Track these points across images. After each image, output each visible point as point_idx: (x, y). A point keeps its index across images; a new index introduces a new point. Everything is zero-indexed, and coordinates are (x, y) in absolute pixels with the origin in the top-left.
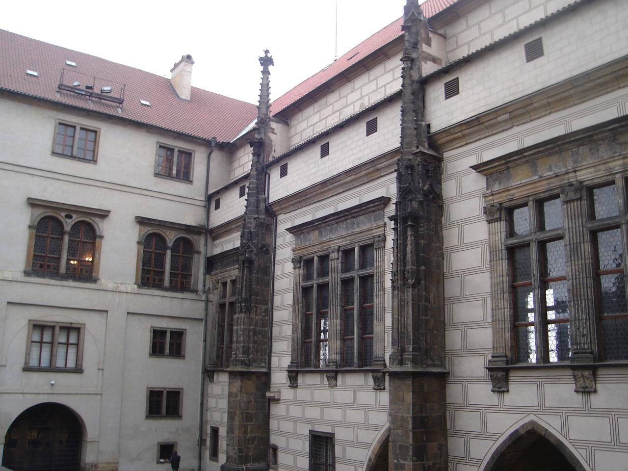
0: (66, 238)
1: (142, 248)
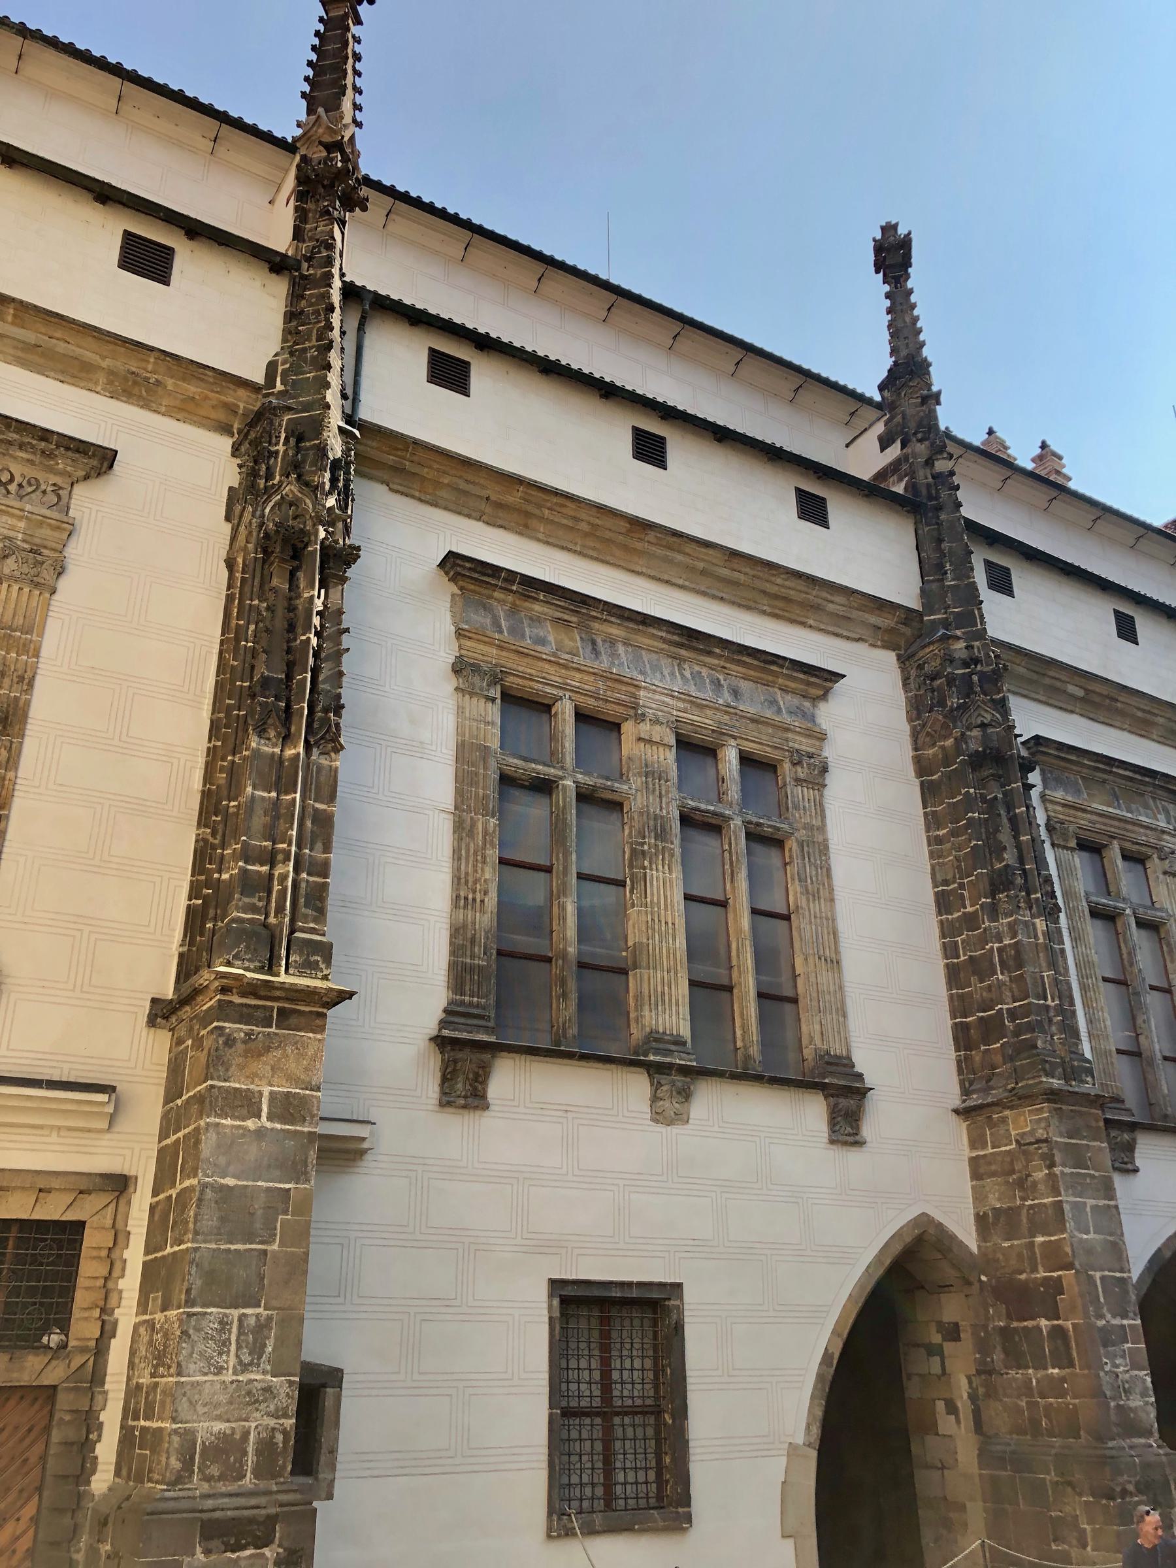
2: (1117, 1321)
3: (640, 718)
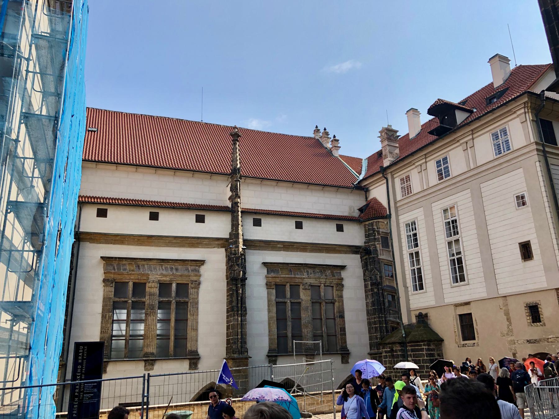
3: (149, 282)
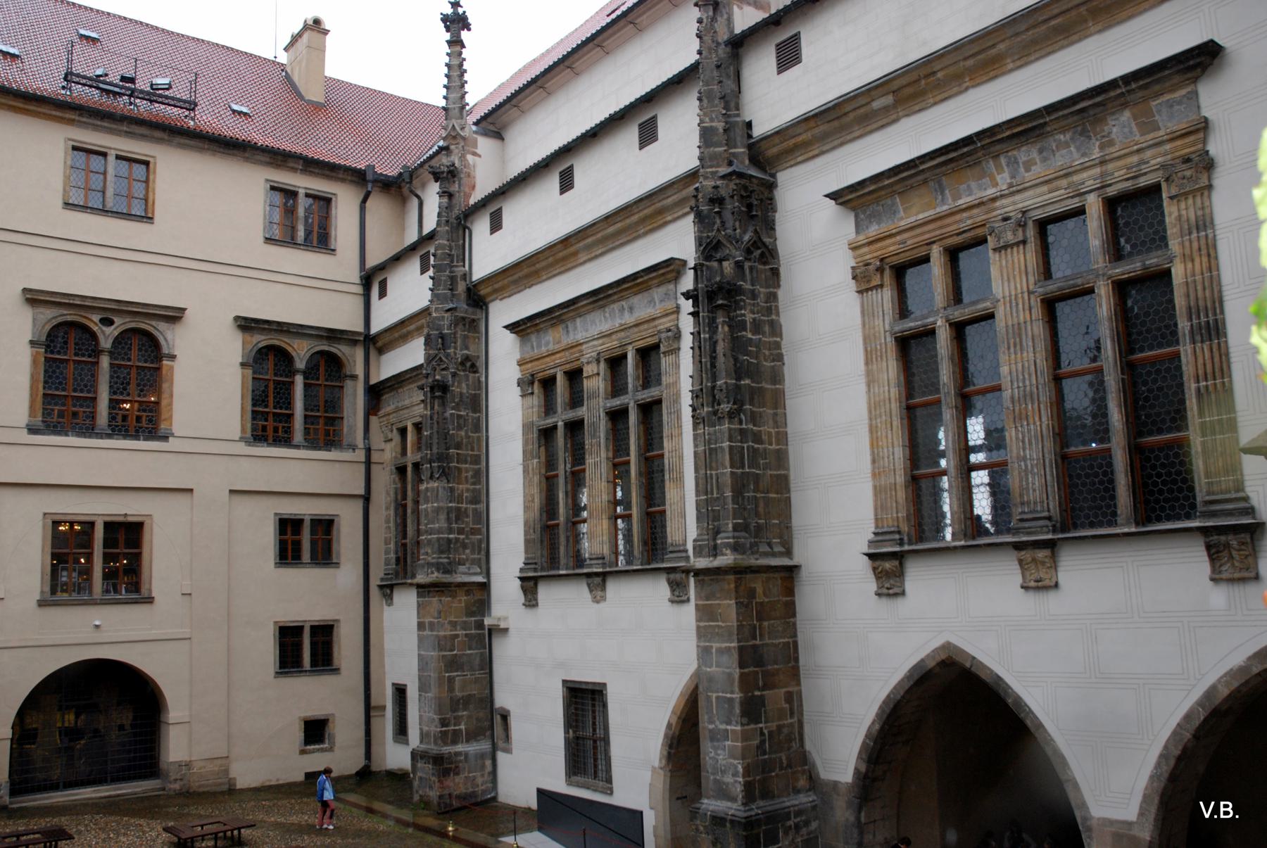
0: (105, 361)
1: (249, 372)
2: (723, 727)
